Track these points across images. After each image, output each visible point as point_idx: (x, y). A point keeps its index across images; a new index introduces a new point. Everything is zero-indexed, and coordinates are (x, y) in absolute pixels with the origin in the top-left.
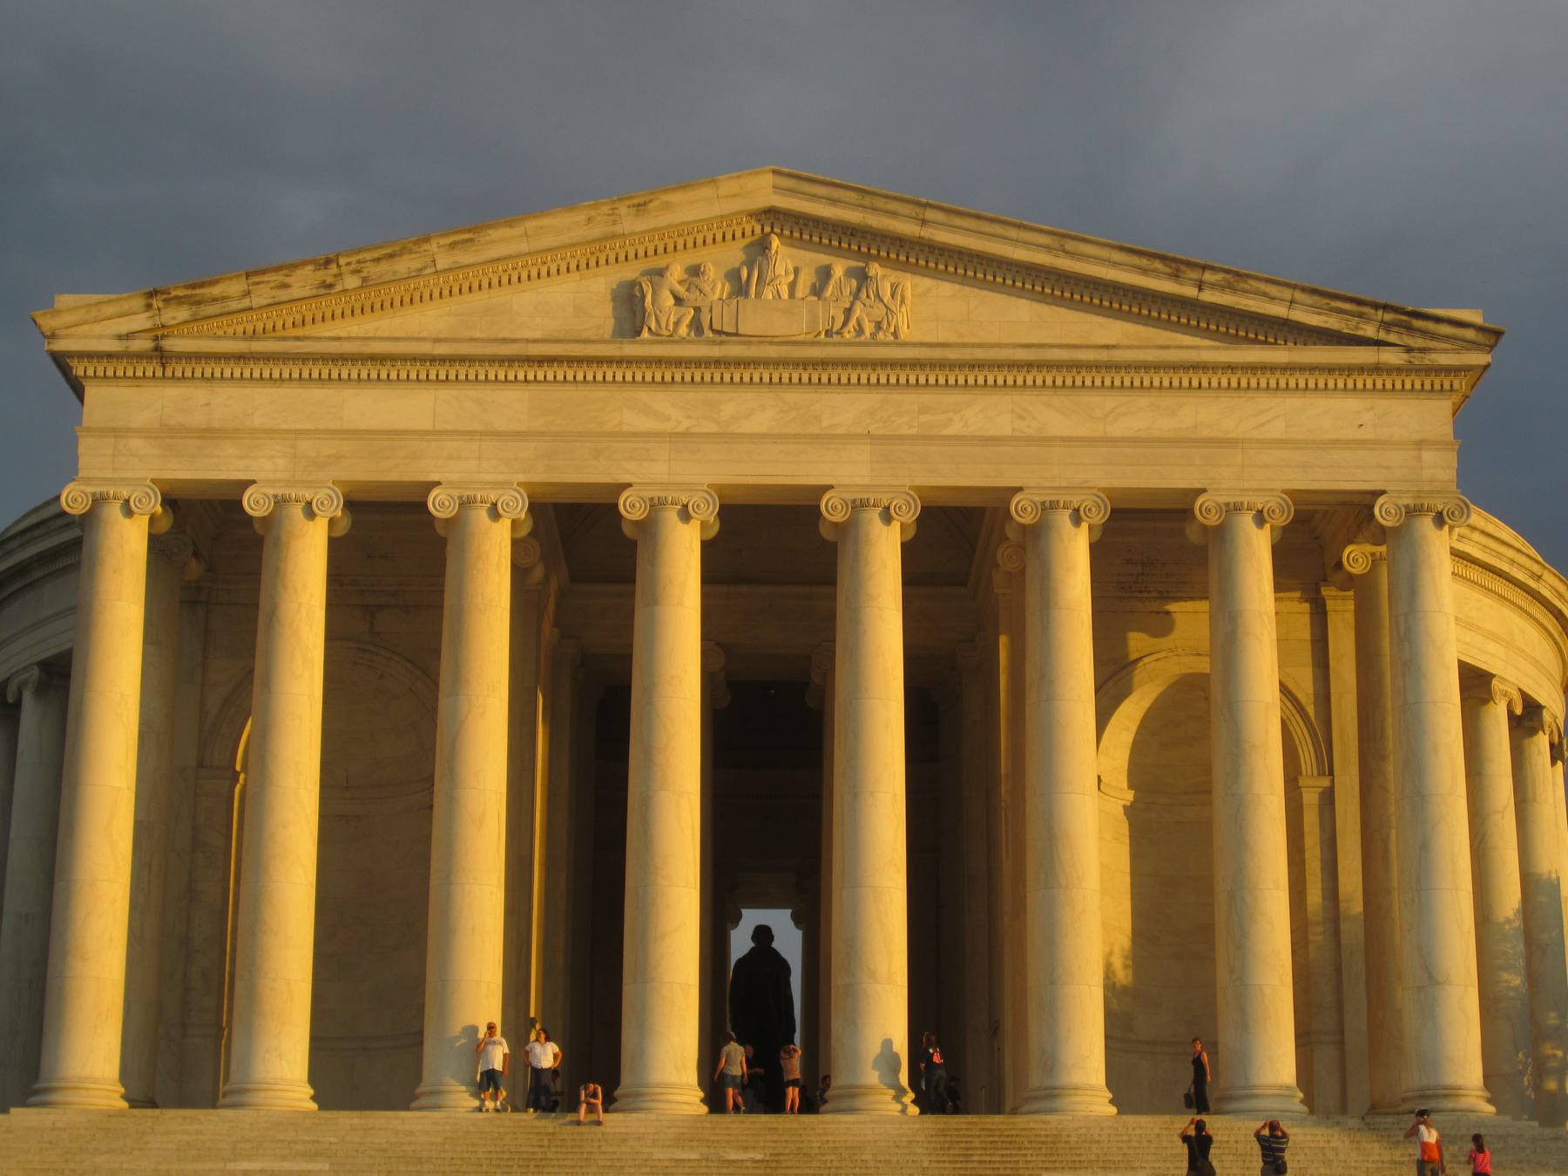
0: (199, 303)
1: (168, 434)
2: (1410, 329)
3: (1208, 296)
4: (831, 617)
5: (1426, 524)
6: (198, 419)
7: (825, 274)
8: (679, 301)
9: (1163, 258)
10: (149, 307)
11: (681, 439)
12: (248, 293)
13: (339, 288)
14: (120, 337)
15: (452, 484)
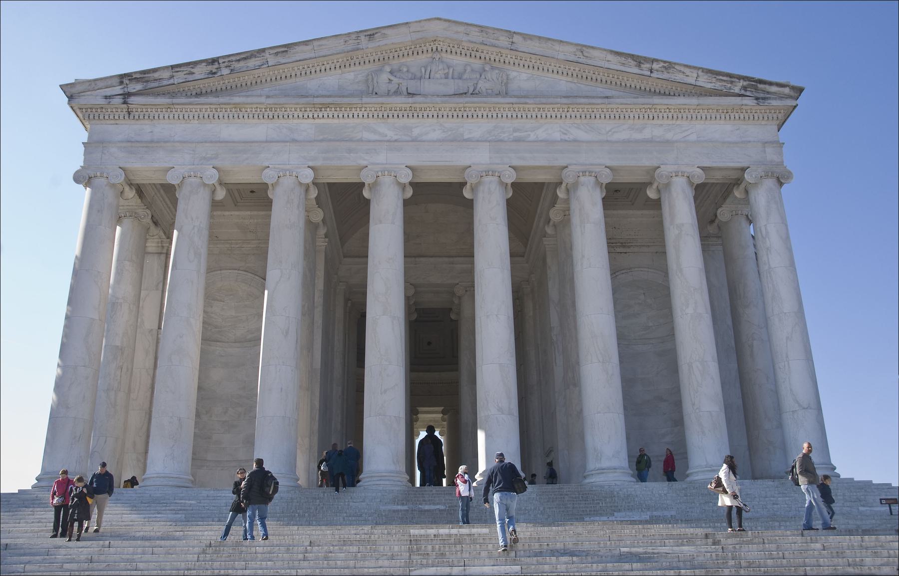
0: (147, 81)
1: (132, 145)
2: (756, 89)
4: (470, 272)
5: (770, 183)
9: (632, 56)
10: (121, 83)
12: (172, 77)
13: (219, 74)
14: (106, 97)
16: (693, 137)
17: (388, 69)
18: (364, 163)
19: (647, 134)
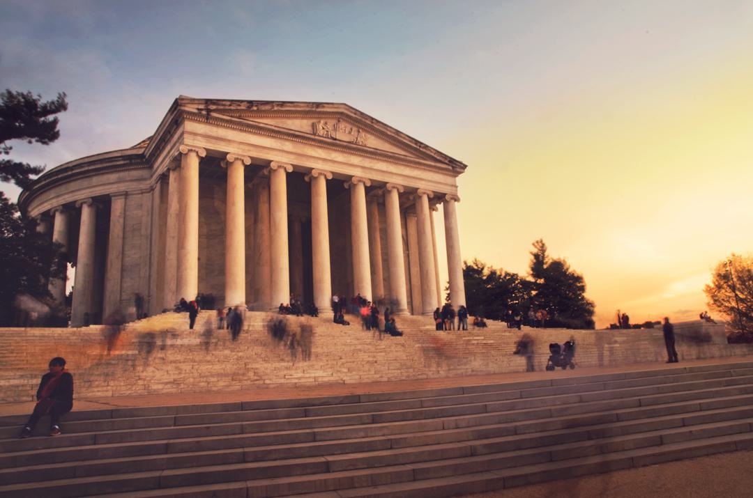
0: (219, 105)
1: (207, 137)
3: (421, 149)
6: (214, 134)
7: (352, 130)
8: (323, 128)
10: (206, 103)
11: (324, 160)
12: (230, 105)
14: (198, 109)
15: (276, 162)
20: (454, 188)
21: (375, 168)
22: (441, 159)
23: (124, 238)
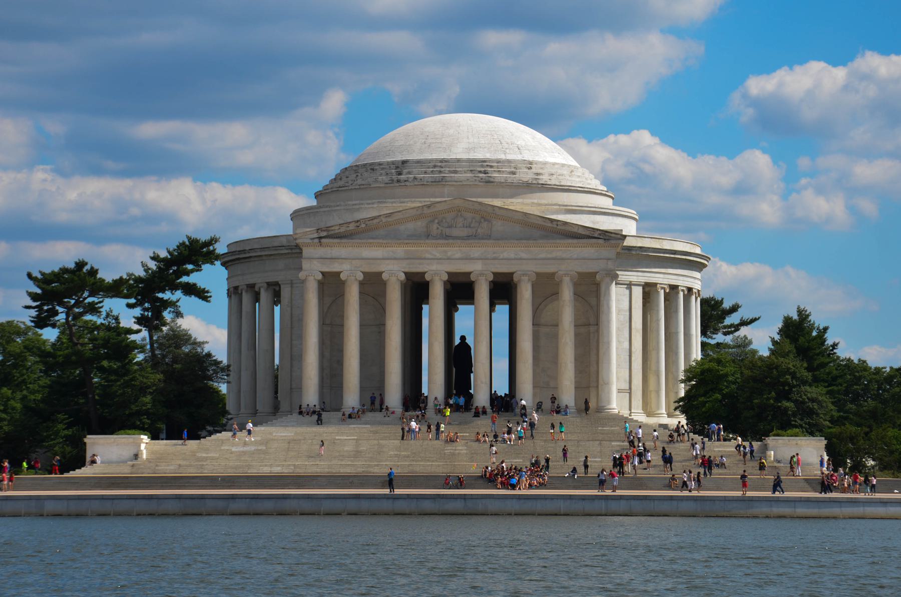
16: (575, 256)
17: (436, 221)
18: (426, 270)
19: (554, 255)
20: (610, 263)
21: (501, 257)
22: (587, 233)
23: (292, 328)
